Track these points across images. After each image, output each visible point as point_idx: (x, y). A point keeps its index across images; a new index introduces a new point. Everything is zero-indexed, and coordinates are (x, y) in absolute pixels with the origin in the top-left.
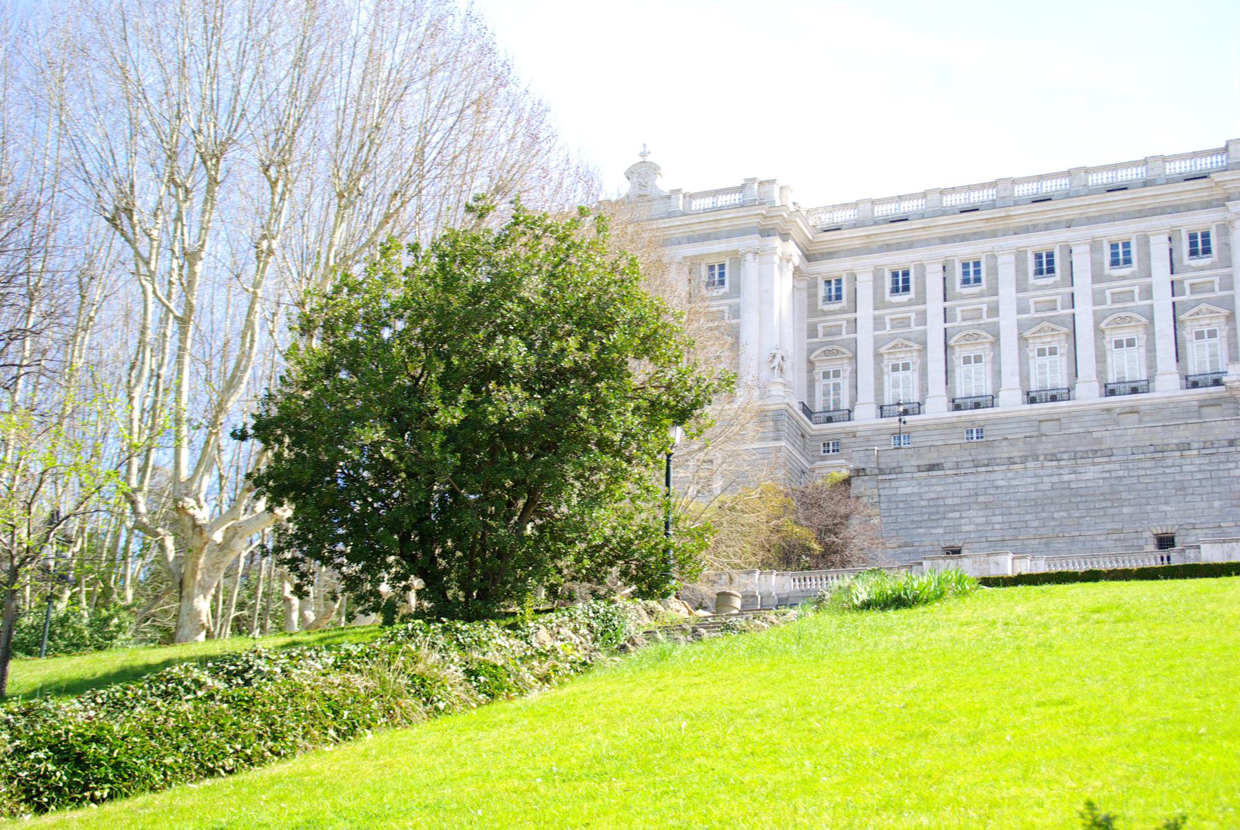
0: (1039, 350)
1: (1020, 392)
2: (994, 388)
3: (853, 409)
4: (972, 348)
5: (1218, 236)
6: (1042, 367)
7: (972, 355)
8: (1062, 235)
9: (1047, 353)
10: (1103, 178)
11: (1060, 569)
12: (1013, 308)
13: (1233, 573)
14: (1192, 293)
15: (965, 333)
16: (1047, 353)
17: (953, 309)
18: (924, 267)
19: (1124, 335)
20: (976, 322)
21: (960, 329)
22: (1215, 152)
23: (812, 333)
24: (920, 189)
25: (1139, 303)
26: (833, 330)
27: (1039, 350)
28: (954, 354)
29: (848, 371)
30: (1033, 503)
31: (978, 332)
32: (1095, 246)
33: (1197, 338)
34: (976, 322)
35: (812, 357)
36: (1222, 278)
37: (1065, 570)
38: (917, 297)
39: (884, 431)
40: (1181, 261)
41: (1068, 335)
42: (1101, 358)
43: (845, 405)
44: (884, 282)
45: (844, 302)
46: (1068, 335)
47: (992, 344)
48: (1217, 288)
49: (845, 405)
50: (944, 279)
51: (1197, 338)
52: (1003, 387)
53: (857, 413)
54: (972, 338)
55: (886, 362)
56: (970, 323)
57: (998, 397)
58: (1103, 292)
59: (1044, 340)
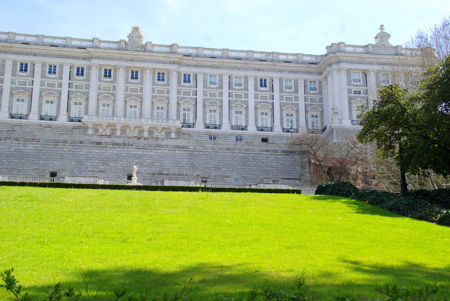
0: (75, 102)
1: (66, 117)
2: (245, 124)
3: (29, 115)
4: (264, 110)
5: (114, 71)
6: (104, 110)
7: (106, 104)
8: (32, 58)
9: (78, 104)
10: (49, 41)
11: (41, 182)
12: (250, 96)
13: (135, 189)
14: (157, 93)
15: (158, 98)
16: (78, 104)
17: (72, 84)
18: (222, 77)
19: (213, 108)
20: (108, 92)
21: (208, 99)
22: (167, 46)
23: (321, 100)
24: (36, 34)
25: (218, 97)
26: (51, 85)
27: (75, 102)
28: (232, 109)
29: (57, 102)
30: (114, 160)
31: (163, 99)
32: (44, 65)
33: (184, 111)
34: (108, 92)
35: (99, 97)
36: (193, 91)
37: (43, 182)
38: (244, 88)
39: (259, 136)
40: (73, 76)
41: (194, 105)
42: (256, 119)
43: (218, 123)
44: (17, 67)
45: (166, 82)
46: (194, 105)
47: (86, 99)
48: (84, 88)
49: (295, 127)
50: (70, 72)
51: (184, 111)
52: (249, 124)
53: (249, 127)
54: (213, 103)
55: (259, 111)
56: (105, 92)
57: (221, 126)
58: (44, 82)
59: (77, 99)
